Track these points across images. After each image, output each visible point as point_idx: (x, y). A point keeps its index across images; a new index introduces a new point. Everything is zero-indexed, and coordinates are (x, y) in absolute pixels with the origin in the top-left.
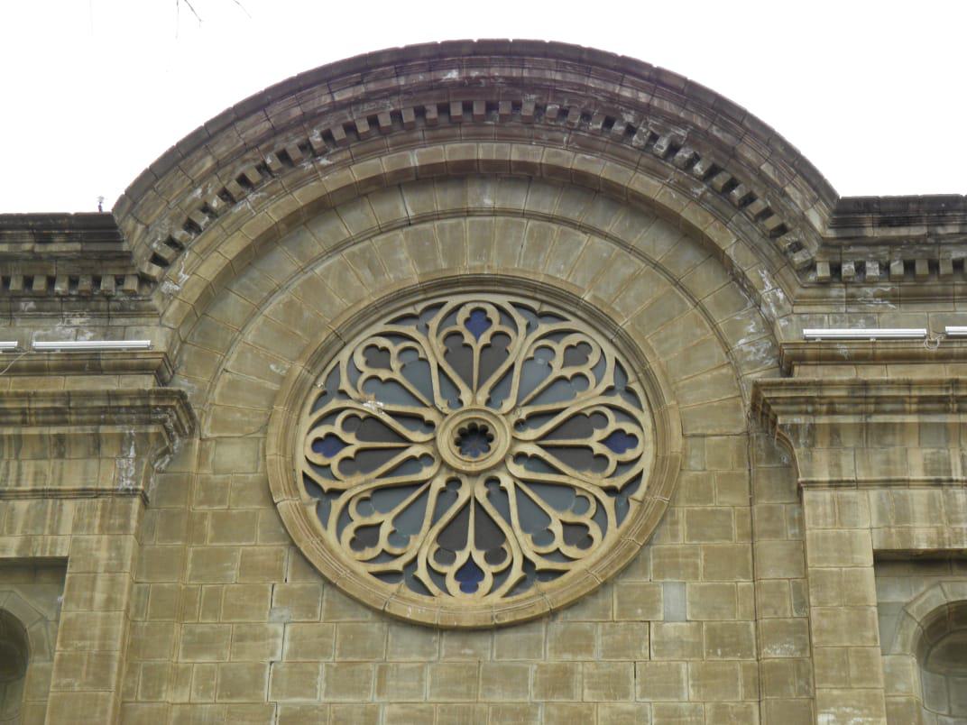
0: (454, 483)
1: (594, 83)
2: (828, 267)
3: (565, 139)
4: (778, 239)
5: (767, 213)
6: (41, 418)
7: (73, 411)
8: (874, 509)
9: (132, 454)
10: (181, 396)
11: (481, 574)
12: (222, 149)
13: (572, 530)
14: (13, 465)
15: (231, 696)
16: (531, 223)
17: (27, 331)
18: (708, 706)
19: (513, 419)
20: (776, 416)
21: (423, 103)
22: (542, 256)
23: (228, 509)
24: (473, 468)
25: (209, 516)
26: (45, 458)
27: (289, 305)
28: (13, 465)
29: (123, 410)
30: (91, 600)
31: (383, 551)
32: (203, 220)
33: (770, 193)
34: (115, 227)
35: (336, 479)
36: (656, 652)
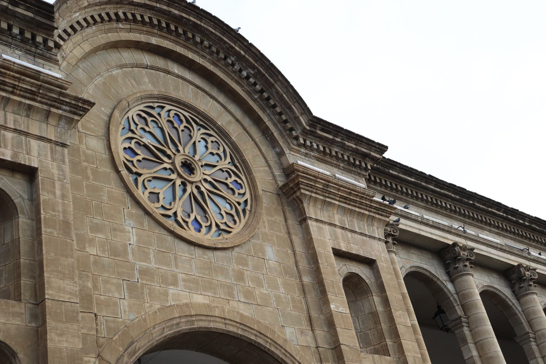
6: (22, 93)
7: (40, 95)
11: (201, 226)
15: (115, 256)
16: (191, 86)
18: (289, 296)
20: (299, 189)
21: (160, 19)
22: (198, 101)
23: (97, 168)
24: (190, 179)
25: (89, 168)
27: (104, 83)
30: (54, 194)
31: (162, 206)
34: (53, 13)
36: (269, 271)
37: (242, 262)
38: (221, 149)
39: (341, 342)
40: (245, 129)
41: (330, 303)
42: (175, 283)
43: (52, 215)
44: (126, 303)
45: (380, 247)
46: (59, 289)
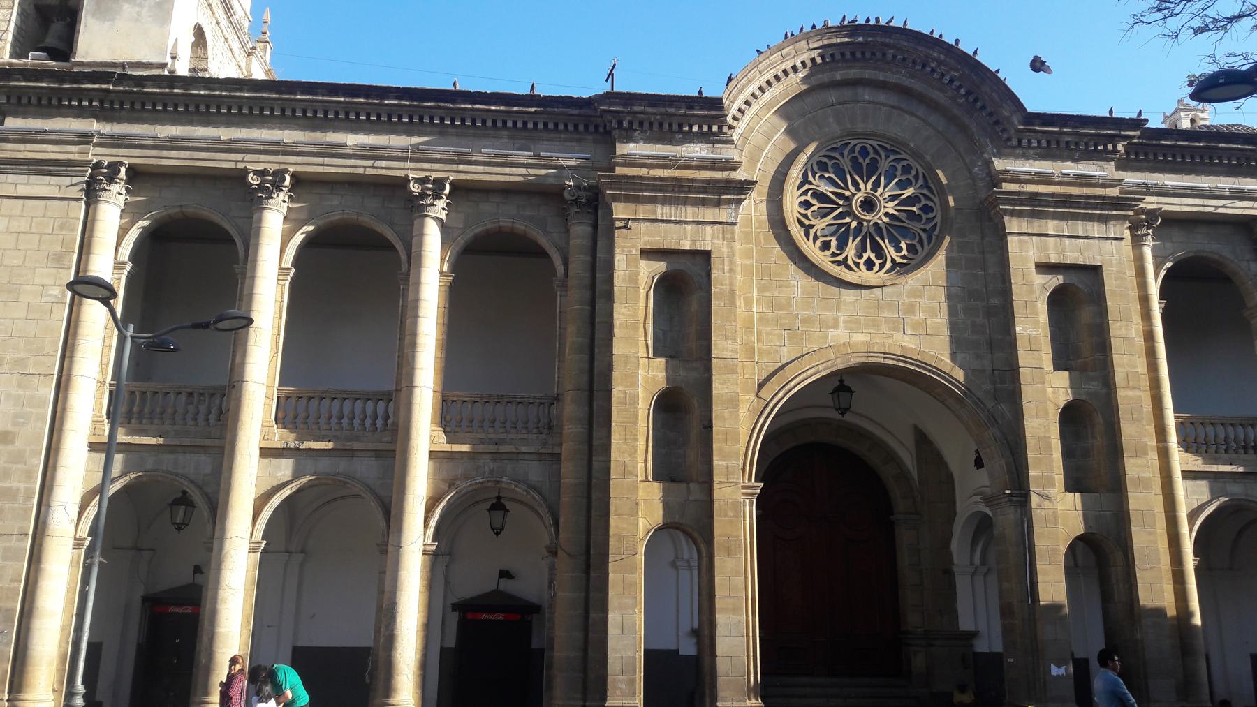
9: (733, 207)
16: (885, 108)
20: (998, 204)
28: (683, 209)
30: (724, 269)
31: (833, 252)
38: (914, 172)
39: (1020, 365)
41: (1016, 325)
42: (835, 325)
44: (785, 349)
46: (724, 349)
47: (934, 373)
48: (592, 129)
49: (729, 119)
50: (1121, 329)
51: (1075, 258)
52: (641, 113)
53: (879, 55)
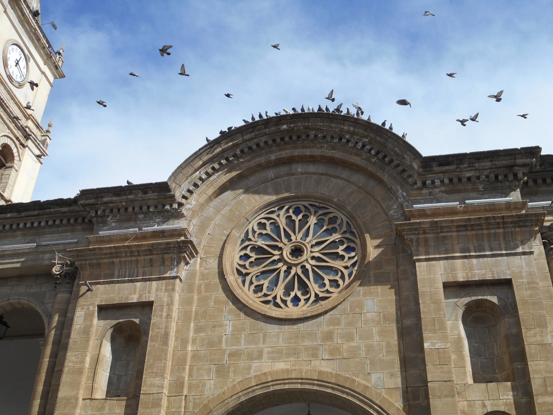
0: (289, 268)
1: (334, 125)
2: (421, 182)
3: (325, 146)
4: (402, 174)
5: (398, 165)
6: (144, 253)
7: (155, 250)
8: (442, 268)
9: (175, 264)
10: (191, 242)
12: (205, 158)
13: (332, 283)
14: (136, 270)
15: (211, 347)
17: (141, 225)
19: (310, 245)
20: (404, 236)
22: (319, 188)
24: (296, 262)
26: (146, 267)
27: (231, 210)
28: (136, 270)
29: (172, 249)
30: (162, 315)
31: (265, 293)
32: (199, 183)
33: (399, 158)
34: (169, 186)
35: (248, 269)
36: (364, 324)
37: (336, 322)
39: (429, 380)
40: (367, 193)
42: (260, 356)
43: (157, 333)
44: (212, 382)
45: (523, 261)
46: (152, 385)
47: (348, 394)
48: (80, 220)
49: (178, 198)
50: (535, 336)
51: (484, 275)
52: (111, 202)
53: (303, 137)
